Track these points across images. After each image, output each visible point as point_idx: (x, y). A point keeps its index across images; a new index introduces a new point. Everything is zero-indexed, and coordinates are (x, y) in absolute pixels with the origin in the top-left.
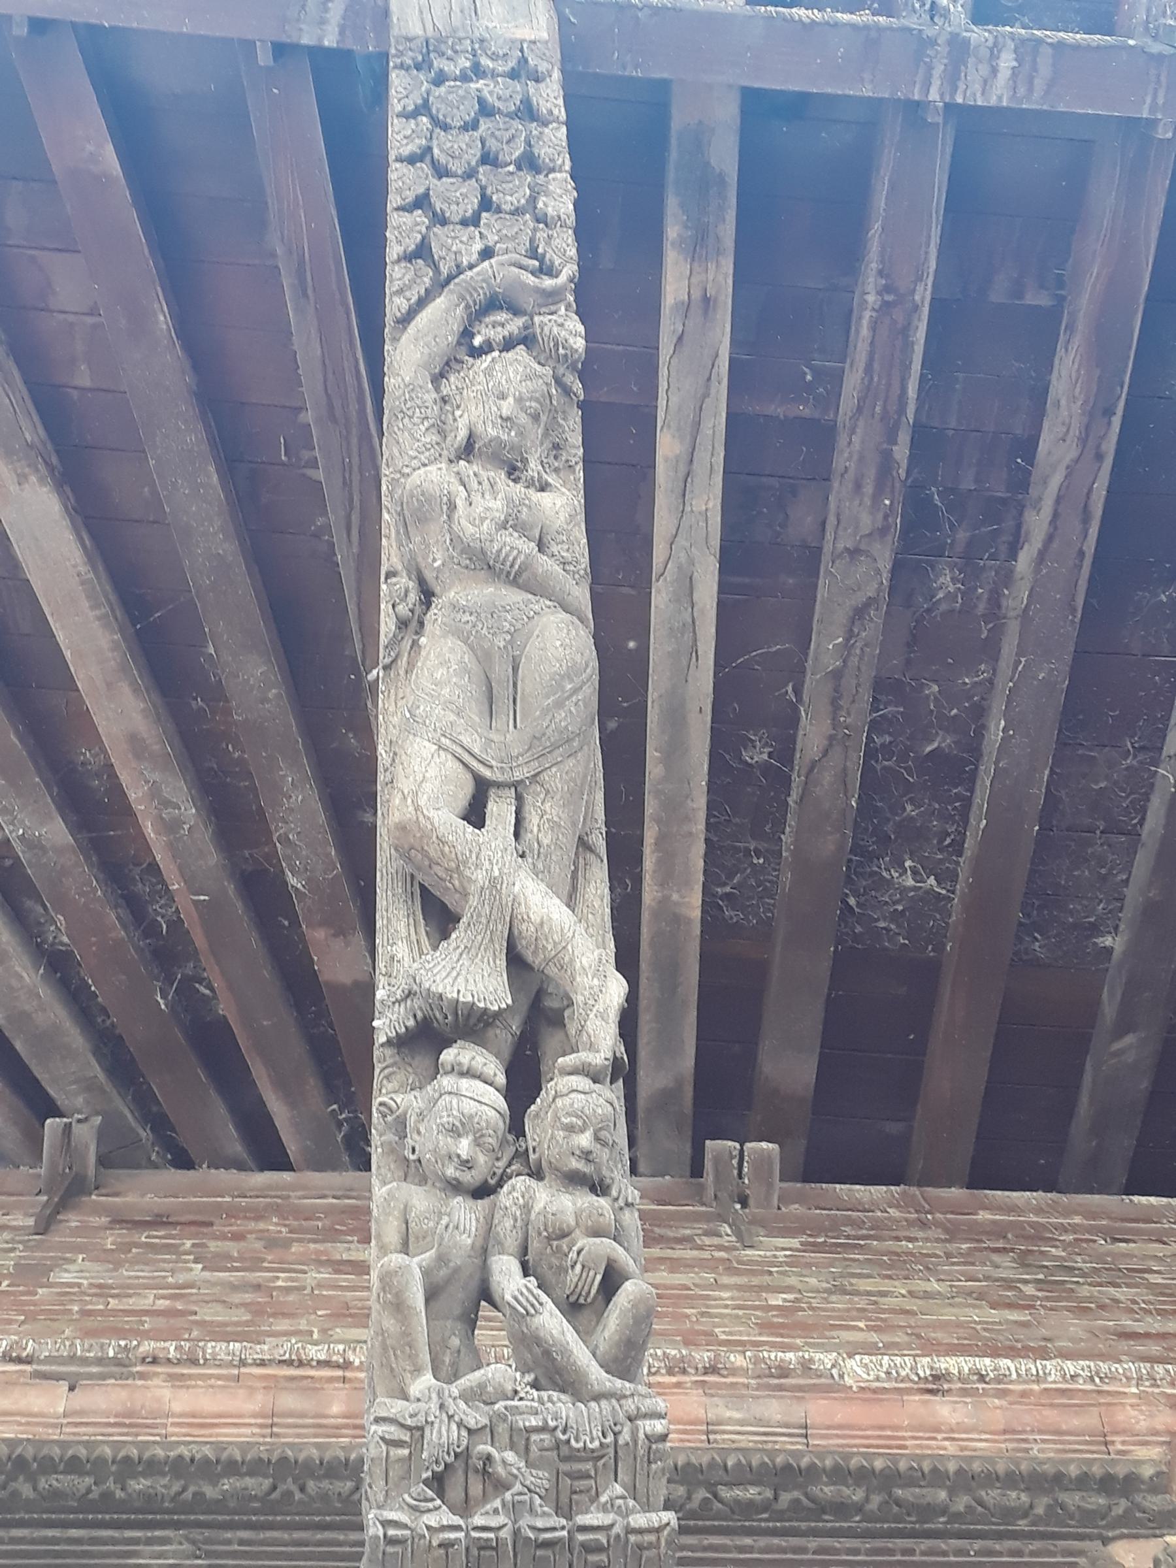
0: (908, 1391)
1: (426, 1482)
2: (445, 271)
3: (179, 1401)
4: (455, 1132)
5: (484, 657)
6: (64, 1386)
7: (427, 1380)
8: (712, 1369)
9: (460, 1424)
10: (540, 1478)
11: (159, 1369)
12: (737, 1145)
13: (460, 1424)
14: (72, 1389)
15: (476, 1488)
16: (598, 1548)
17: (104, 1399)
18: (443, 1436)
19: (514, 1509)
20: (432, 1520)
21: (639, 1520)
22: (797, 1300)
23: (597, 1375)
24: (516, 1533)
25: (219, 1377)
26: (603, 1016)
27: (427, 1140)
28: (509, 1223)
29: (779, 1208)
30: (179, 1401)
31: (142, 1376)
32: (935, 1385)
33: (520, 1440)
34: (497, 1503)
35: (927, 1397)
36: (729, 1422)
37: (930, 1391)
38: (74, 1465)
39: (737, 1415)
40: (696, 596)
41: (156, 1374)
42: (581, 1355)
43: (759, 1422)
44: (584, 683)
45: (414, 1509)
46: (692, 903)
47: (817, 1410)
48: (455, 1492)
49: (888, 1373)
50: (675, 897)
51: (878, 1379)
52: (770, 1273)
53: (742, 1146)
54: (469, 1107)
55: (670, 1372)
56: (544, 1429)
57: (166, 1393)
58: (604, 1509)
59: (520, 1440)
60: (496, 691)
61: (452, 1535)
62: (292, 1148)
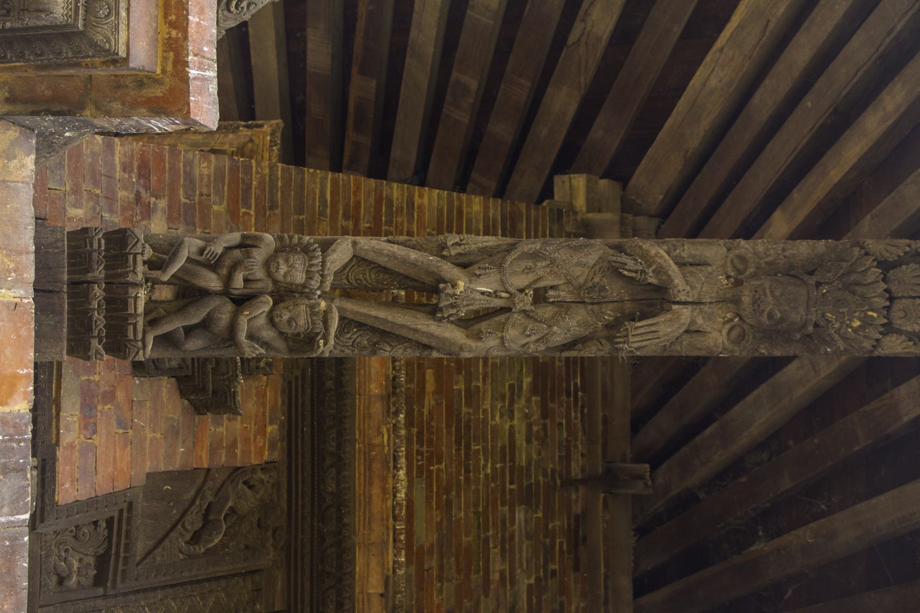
6: (381, 591)
14: (382, 595)
62: (645, 600)
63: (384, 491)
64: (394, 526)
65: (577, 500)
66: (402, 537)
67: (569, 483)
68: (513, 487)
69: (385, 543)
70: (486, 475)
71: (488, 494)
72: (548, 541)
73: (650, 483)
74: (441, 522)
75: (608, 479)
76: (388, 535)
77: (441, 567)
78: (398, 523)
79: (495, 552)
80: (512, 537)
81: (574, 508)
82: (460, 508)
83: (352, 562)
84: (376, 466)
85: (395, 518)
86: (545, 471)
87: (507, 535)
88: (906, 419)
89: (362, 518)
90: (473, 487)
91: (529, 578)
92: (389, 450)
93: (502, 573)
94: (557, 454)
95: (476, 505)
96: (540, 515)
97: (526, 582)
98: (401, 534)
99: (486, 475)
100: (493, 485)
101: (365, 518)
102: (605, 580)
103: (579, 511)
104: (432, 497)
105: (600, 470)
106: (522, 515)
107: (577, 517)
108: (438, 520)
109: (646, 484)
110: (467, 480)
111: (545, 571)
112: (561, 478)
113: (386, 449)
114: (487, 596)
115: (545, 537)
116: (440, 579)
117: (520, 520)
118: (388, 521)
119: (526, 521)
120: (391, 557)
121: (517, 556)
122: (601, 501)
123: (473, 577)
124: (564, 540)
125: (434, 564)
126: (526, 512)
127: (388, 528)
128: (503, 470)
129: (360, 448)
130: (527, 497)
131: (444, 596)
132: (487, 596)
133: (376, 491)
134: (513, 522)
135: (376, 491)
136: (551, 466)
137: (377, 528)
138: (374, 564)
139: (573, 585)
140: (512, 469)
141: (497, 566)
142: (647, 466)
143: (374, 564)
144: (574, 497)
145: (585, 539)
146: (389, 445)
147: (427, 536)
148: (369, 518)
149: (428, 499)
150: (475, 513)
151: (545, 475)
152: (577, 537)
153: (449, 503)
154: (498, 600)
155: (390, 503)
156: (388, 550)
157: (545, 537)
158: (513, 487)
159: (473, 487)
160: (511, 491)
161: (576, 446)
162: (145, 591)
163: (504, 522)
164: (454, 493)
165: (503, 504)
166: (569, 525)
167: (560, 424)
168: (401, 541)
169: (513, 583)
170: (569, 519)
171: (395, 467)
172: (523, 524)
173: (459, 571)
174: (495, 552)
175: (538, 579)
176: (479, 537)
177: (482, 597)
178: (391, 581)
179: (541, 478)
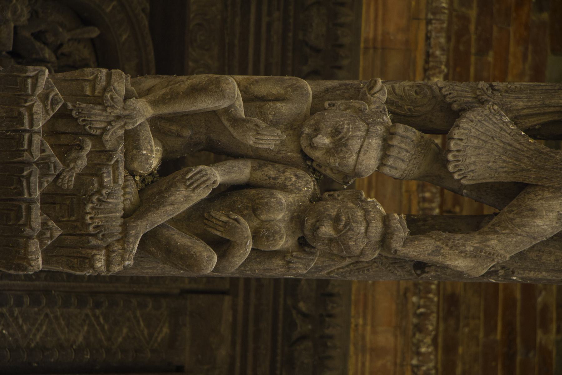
4: (336, 132)
10: (69, 182)
13: (104, 130)
15: (64, 140)
16: (19, 218)
18: (97, 118)
19: (44, 165)
20: (38, 107)
24: (29, 164)
26: (437, 251)
33: (94, 170)
48: (61, 126)
54: (355, 145)
56: (102, 185)
58: (44, 224)
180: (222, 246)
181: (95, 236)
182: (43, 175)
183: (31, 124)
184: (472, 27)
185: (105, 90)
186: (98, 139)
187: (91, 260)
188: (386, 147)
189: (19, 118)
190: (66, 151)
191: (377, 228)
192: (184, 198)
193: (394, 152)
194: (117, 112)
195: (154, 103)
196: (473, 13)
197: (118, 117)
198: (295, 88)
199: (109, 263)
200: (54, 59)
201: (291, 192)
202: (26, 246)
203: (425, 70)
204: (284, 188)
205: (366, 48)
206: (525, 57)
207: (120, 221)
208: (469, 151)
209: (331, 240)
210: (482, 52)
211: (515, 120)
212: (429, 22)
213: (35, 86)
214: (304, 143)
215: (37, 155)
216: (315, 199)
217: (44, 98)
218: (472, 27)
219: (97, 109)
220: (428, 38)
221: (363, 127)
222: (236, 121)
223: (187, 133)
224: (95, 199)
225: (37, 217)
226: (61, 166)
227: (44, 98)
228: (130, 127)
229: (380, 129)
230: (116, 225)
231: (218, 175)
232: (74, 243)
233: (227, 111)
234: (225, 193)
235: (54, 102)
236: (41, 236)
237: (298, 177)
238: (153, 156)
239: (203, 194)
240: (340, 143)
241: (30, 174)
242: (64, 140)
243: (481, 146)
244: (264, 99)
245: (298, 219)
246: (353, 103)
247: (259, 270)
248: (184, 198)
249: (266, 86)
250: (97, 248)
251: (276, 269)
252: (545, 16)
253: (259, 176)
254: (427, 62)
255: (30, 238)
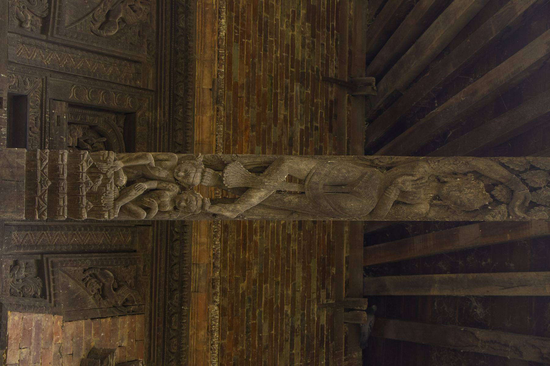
0: (208, 323)
1: (94, 163)
2: (524, 176)
3: (206, 119)
4: (186, 171)
5: (353, 185)
6: (210, 87)
7: (122, 165)
8: (214, 267)
9: (107, 171)
10: (96, 189)
11: (215, 113)
12: (365, 309)
13: (107, 171)
14: (210, 89)
15: (93, 175)
16: (78, 201)
17: (207, 98)
18: (105, 167)
19: (87, 183)
20: (85, 164)
21: (84, 211)
22: (287, 315)
23: (121, 204)
24: (82, 183)
25: (213, 129)
26: (220, 210)
27: (186, 166)
28: (165, 185)
29: (345, 323)
30: (206, 119)
31: (214, 108)
32: (210, 332)
33: (104, 185)
34: (89, 179)
35: (206, 328)
36: (200, 271)
37: (208, 329)
38: (186, 91)
39: (201, 272)
40: (520, 287)
41: (214, 112)
42: (126, 200)
43: (200, 279)
44: (338, 212)
45: (88, 160)
46: (434, 292)
47: (203, 296)
48: (93, 170)
49: (213, 317)
50: (436, 285)
51: (212, 314)
52: (303, 309)
53: (365, 311)
54: (192, 175)
55: (214, 254)
56: (106, 190)
57: (208, 115)
58: (87, 203)
59: (104, 185)
60: (341, 188)
61: (81, 169)
63: (213, 31)
64: (218, 51)
65: (332, 92)
66: (223, 58)
67: (327, 80)
68: (293, 70)
69: (213, 61)
70: (277, 57)
71: (277, 71)
72: (313, 108)
73: (375, 88)
74: (248, 73)
75: (350, 86)
76: (215, 56)
77: (248, 99)
78: (220, 49)
79: (281, 103)
80: (292, 98)
81: (330, 96)
82: (261, 70)
83: (194, 68)
84: (209, 16)
85: (219, 47)
86: (312, 68)
87: (289, 96)
88: (519, 13)
89: (200, 46)
90: (269, 61)
91: (301, 125)
92: (216, 7)
93: (285, 116)
94: (320, 61)
95: (270, 71)
96: (309, 92)
97: (300, 127)
98: (222, 56)
99: (277, 57)
100: (281, 64)
101: (202, 45)
102: (348, 144)
103: (333, 99)
104: (244, 56)
105: (347, 80)
106: (298, 88)
107: (331, 102)
108: (247, 71)
109: (373, 88)
110: (265, 55)
111: (312, 125)
112: (322, 75)
113: (215, 6)
114: (276, 126)
115: (312, 106)
116: (248, 106)
117: (297, 91)
118: (215, 48)
119: (300, 92)
120: (216, 68)
121: (295, 110)
122: (347, 98)
123: (268, 112)
124: (324, 112)
125: (244, 95)
126: (301, 88)
127: (215, 52)
128: (287, 57)
129: (199, 5)
130: (302, 79)
131: (250, 116)
132: (276, 126)
133: (208, 30)
134: (292, 90)
135: (208, 30)
136: (316, 66)
137: (209, 52)
138: (206, 72)
139: (328, 139)
140: (293, 59)
141: (282, 112)
142: (374, 79)
143: (206, 72)
144: (330, 89)
145: (336, 116)
146: (216, 4)
147: (240, 78)
148: (204, 46)
149: (241, 57)
150: (270, 76)
151: (313, 71)
152: (332, 112)
153: (254, 64)
154: (282, 130)
155: (216, 37)
156: (214, 64)
157: (312, 106)
158: (293, 70)
159: (269, 61)
160: (292, 72)
161: (332, 61)
162: (71, 47)
163: (287, 88)
164: (257, 60)
165: (287, 77)
166: (327, 104)
167: (323, 45)
168: (222, 60)
169: (292, 124)
170: (327, 100)
171: (219, 17)
172: (298, 94)
173: (259, 105)
174: (281, 103)
175: (307, 128)
176: (272, 90)
177: (273, 126)
178: (216, 82)
179: (310, 71)
180: (148, 210)
181: (104, 207)
182: (87, 187)
183: (82, 170)
184: (231, 137)
185: (107, 158)
186: (105, 174)
187: (104, 215)
188: (203, 176)
189: (78, 168)
190: (94, 179)
191: (200, 203)
192: (134, 194)
193: (205, 177)
194: (112, 165)
195: (124, 162)
196: (231, 132)
197: (112, 167)
198: (172, 157)
199: (109, 216)
200: (91, 148)
201: (171, 191)
202: (81, 211)
203: (216, 151)
204: (168, 190)
205: (196, 144)
206: (248, 146)
207: (113, 202)
208: (230, 177)
209: (185, 207)
210: (234, 145)
211: (245, 166)
212: (217, 135)
213: (83, 157)
214: (175, 175)
215: (85, 180)
216: (179, 193)
217: (87, 161)
218: (231, 137)
219: (105, 165)
220: (216, 140)
221: (195, 169)
222: (152, 168)
223: (135, 172)
224: (104, 195)
225: (85, 200)
226: (92, 184)
227: (87, 161)
228: (116, 170)
229: (200, 170)
230: (112, 203)
231: (146, 186)
232: (98, 210)
233: (149, 164)
234: (148, 192)
235: (90, 162)
236: (86, 207)
237: (173, 186)
238: (124, 180)
239: (141, 192)
240: (187, 175)
241: (82, 187)
242: (93, 175)
243: (234, 175)
244: (161, 160)
245: (173, 200)
246: (191, 161)
247: (160, 218)
248: (134, 194)
249: (162, 156)
250: (105, 211)
251: (166, 217)
252: (254, 133)
253: (160, 186)
254: (216, 148)
255: (82, 208)
